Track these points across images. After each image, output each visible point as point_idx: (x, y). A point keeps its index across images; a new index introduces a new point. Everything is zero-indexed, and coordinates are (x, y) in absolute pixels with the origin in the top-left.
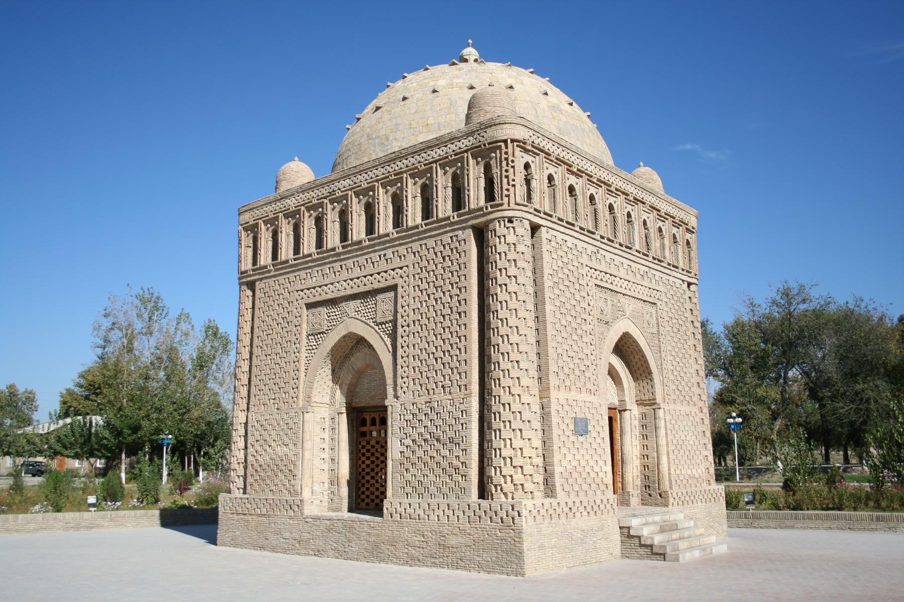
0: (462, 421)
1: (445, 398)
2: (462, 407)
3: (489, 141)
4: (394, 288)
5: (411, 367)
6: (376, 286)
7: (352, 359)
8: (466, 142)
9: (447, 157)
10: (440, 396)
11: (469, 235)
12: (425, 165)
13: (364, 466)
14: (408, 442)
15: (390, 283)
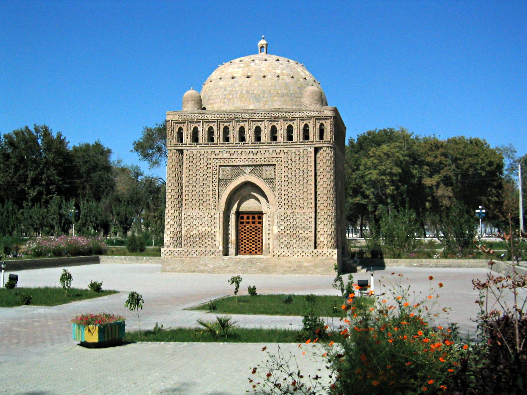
0: (309, 221)
1: (301, 212)
2: (309, 216)
3: (325, 115)
4: (274, 165)
5: (283, 199)
6: (264, 163)
7: (241, 191)
8: (313, 113)
9: (304, 117)
10: (297, 210)
11: (313, 150)
12: (292, 118)
13: (243, 236)
14: (282, 227)
15: (271, 163)
